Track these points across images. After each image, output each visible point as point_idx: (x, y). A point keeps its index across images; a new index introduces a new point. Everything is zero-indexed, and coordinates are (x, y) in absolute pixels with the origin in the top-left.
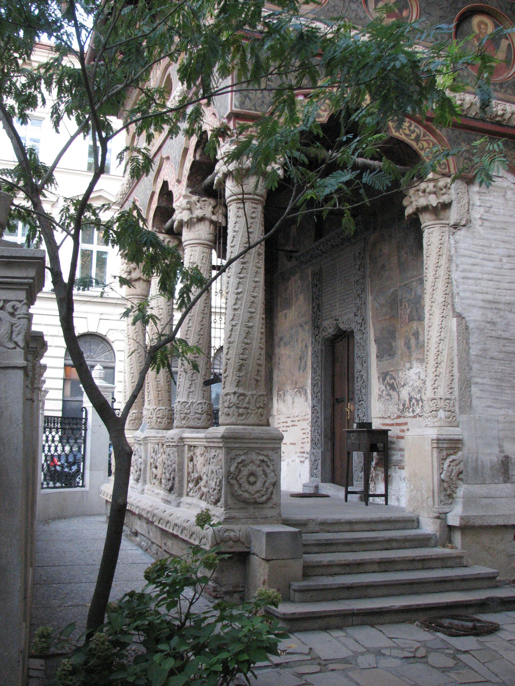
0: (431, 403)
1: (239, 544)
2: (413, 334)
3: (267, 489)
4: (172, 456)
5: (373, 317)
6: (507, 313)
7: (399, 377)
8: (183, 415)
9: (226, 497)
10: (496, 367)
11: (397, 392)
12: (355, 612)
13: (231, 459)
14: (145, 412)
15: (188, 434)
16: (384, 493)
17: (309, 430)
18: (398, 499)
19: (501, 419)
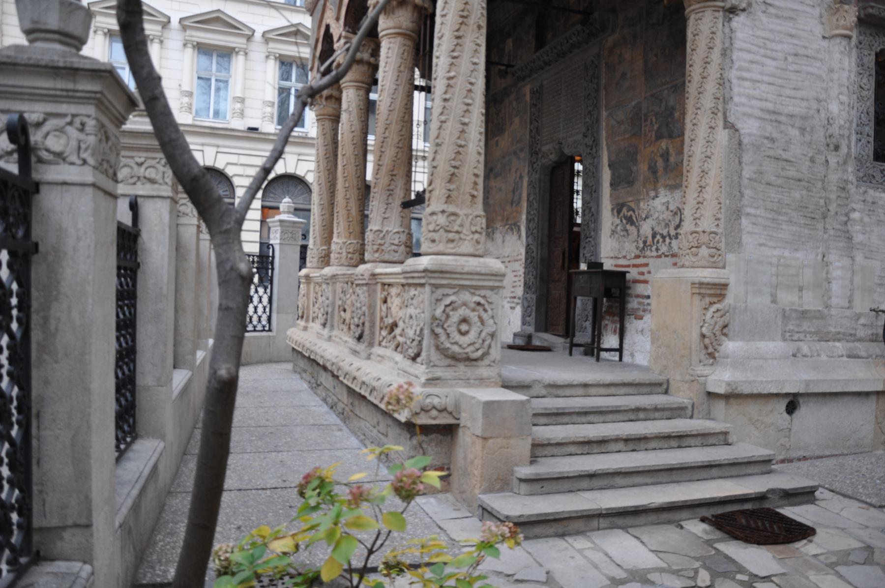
0: (691, 238)
1: (444, 414)
2: (662, 156)
3: (484, 341)
4: (362, 296)
5: (607, 137)
6: (790, 128)
7: (639, 209)
8: (375, 247)
9: (429, 351)
10: (773, 195)
11: (636, 227)
12: (604, 512)
13: (437, 300)
14: (333, 247)
15: (381, 269)
16: (618, 347)
17: (521, 271)
18: (632, 355)
19: (774, 260)
